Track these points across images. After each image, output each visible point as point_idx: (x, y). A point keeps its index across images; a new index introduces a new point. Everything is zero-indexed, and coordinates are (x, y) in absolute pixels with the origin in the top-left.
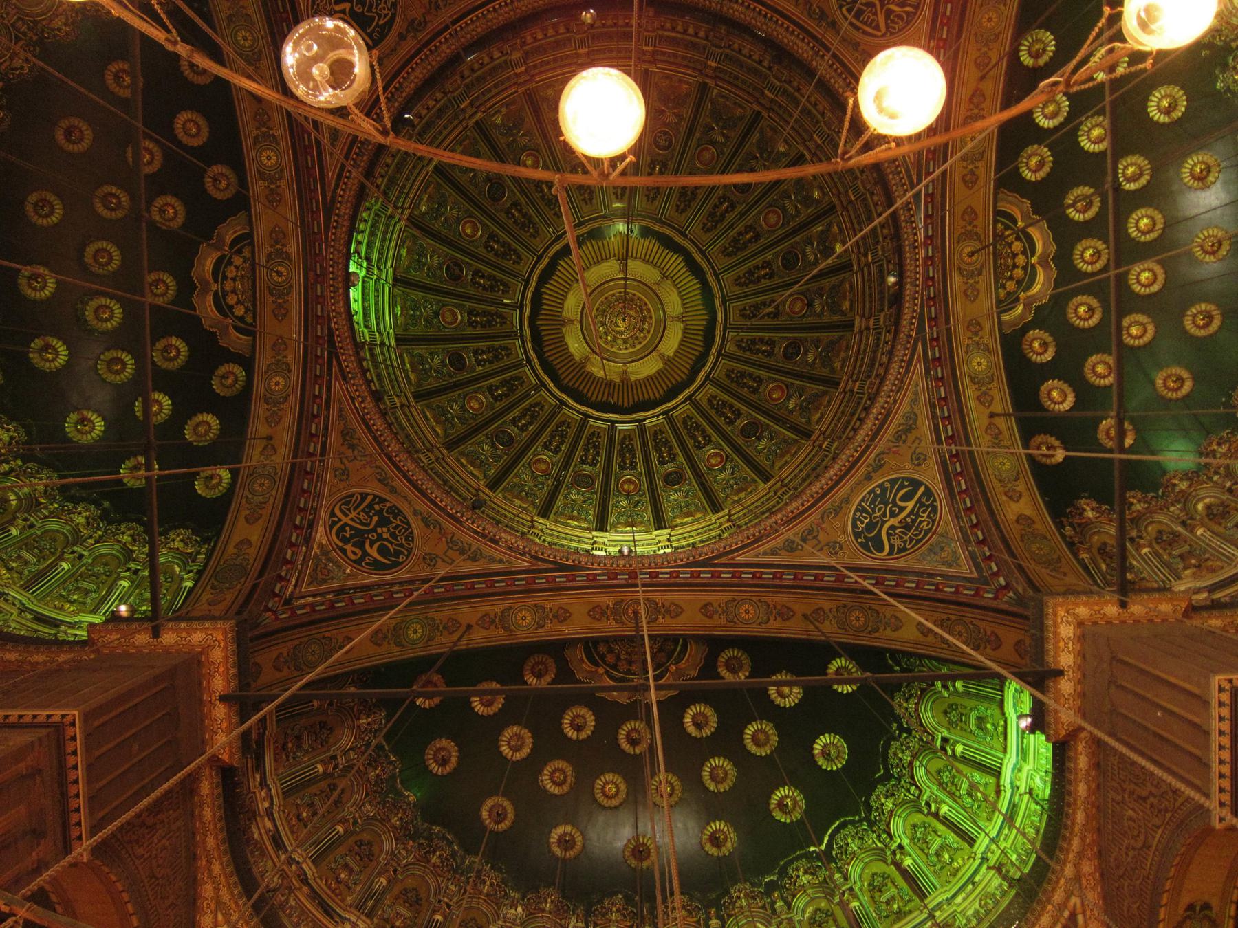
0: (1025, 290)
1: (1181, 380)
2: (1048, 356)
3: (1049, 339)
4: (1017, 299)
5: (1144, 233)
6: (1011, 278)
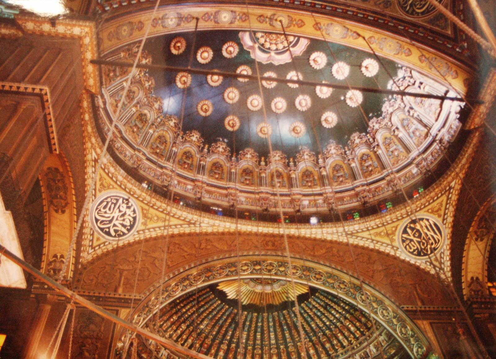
0: (259, 48)
1: (206, 111)
2: (225, 54)
3: (233, 56)
5: (275, 104)
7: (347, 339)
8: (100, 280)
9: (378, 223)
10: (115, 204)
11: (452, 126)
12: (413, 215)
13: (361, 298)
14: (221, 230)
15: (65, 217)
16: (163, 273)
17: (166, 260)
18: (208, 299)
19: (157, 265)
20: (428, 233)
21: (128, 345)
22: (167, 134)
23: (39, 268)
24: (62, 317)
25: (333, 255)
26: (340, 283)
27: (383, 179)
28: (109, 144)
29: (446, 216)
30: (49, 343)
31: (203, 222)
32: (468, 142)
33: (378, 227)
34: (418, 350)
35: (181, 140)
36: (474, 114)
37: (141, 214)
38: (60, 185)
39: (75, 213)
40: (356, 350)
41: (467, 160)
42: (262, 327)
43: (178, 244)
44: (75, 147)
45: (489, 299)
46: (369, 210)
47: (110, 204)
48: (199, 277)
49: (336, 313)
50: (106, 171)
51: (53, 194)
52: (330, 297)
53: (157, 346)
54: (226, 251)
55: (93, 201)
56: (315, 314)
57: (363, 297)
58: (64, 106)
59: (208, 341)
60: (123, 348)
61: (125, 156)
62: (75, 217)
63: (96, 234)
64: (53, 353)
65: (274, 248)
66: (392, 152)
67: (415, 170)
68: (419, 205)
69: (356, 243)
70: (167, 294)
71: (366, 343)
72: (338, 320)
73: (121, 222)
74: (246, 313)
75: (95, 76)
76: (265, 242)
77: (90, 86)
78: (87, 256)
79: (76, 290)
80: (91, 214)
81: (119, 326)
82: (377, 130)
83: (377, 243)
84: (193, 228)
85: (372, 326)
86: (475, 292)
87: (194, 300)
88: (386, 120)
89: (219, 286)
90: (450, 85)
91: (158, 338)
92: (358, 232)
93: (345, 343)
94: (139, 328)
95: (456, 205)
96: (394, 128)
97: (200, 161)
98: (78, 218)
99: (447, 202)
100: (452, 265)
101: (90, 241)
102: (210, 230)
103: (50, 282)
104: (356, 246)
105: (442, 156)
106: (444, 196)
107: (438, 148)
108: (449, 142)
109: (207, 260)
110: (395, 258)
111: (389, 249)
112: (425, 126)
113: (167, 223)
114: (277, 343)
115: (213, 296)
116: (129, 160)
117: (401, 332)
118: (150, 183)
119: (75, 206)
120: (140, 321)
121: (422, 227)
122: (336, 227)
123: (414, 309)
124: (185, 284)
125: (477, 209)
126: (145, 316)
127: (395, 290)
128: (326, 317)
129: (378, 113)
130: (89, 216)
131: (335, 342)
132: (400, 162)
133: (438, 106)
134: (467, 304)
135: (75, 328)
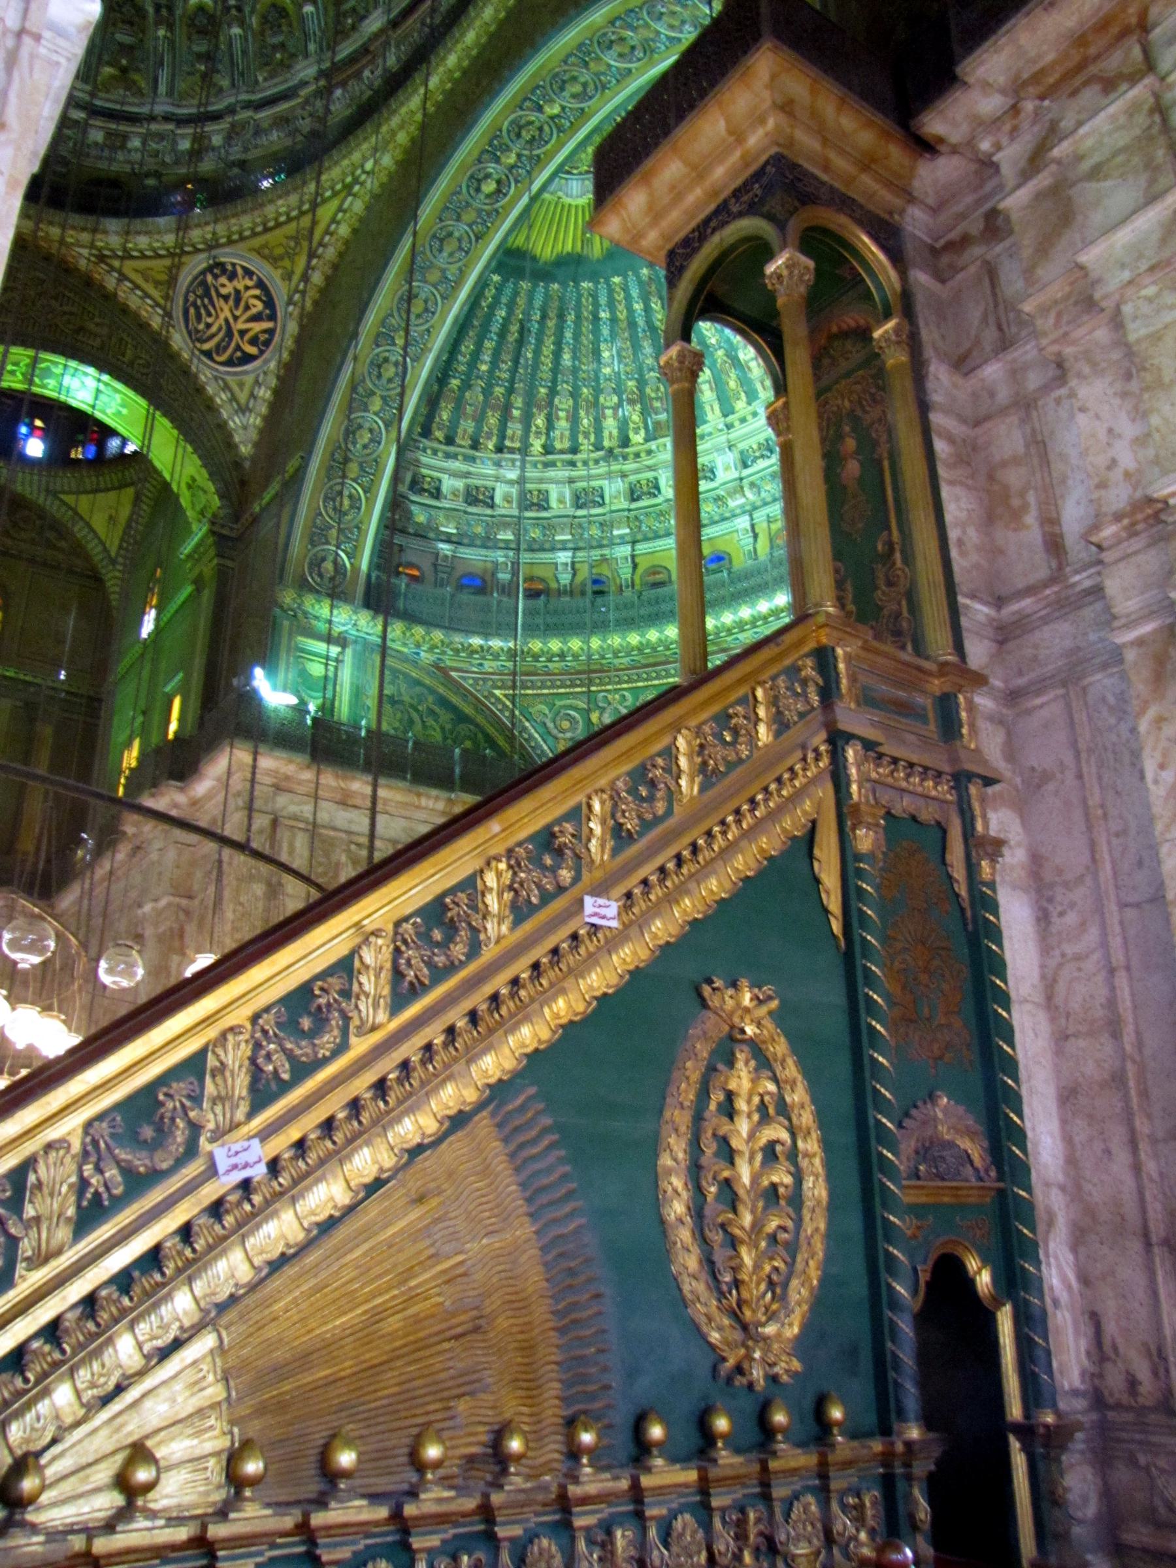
47: (199, 302)
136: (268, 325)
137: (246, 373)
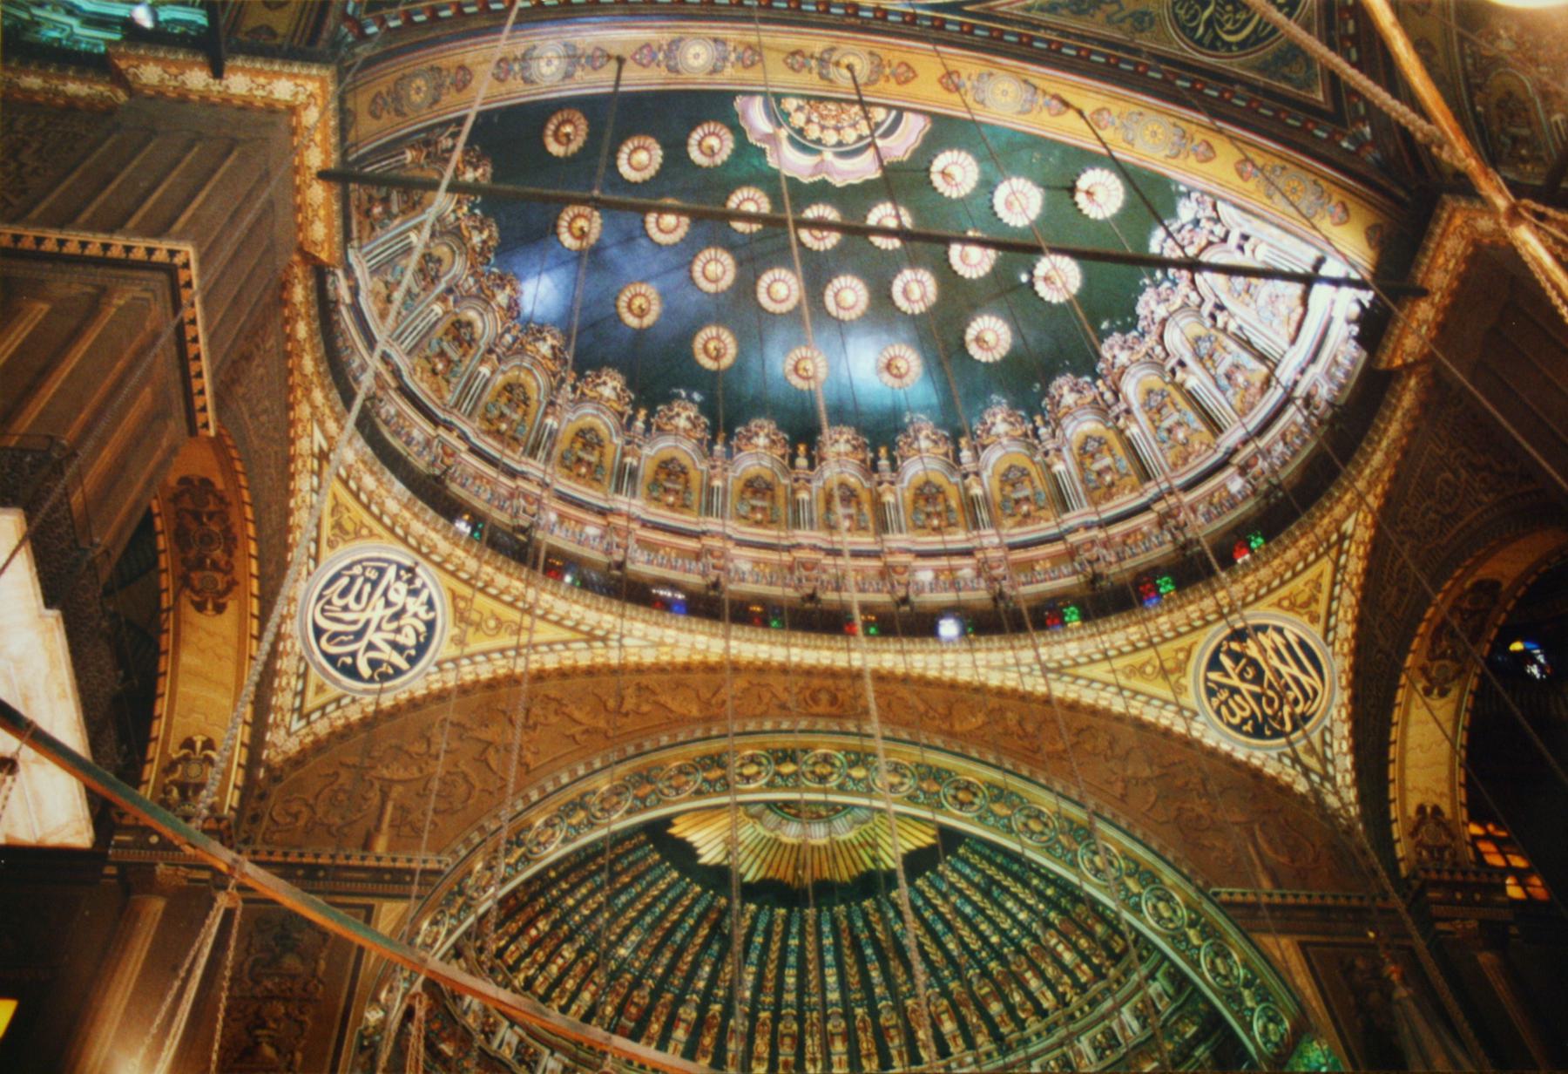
1: (642, 313)
2: (695, 155)
3: (718, 160)
4: (779, 125)
5: (836, 295)
6: (809, 121)
7: (1053, 988)
8: (320, 813)
9: (1134, 638)
10: (375, 584)
11: (1340, 358)
12: (1236, 616)
13: (1092, 862)
14: (681, 657)
15: (225, 624)
16: (511, 788)
17: (521, 748)
18: (642, 868)
19: (493, 764)
20: (1283, 669)
21: (400, 1015)
22: (529, 379)
23: (136, 781)
24: (196, 935)
25: (1007, 733)
26: (1028, 817)
27: (1145, 508)
28: (364, 407)
29: (1333, 621)
30: (151, 1022)
31: (630, 634)
32: (1389, 405)
33: (1136, 649)
34: (1265, 1027)
35: (571, 396)
36: (1400, 324)
37: (450, 610)
38: (215, 528)
39: (256, 611)
40: (1081, 1023)
41: (1387, 454)
42: (802, 948)
43: (554, 699)
44: (264, 418)
45: (1477, 874)
46: (1107, 600)
47: (360, 581)
48: (615, 799)
49: (1020, 905)
50: (353, 485)
51: (192, 554)
52: (999, 859)
53: (488, 1017)
54: (696, 721)
55: (309, 574)
56: (957, 911)
57: (1097, 859)
58: (237, 300)
59: (641, 997)
60: (382, 1025)
61: (408, 443)
62: (255, 624)
63: (314, 673)
64: (164, 1054)
65: (834, 710)
66: (1170, 431)
67: (1236, 485)
68: (1253, 587)
69: (1072, 696)
70: (519, 852)
71: (1108, 1004)
72: (1025, 929)
73: (391, 636)
74: (753, 907)
75: (328, 215)
76: (807, 693)
77: (315, 244)
78: (285, 740)
79: (248, 849)
80: (304, 612)
81: (374, 955)
82: (1124, 369)
83: (1133, 698)
84: (600, 651)
85: (1126, 950)
86: (1431, 853)
87: (601, 869)
88: (1150, 340)
89: (672, 825)
90: (1328, 241)
91: (490, 989)
92: (1077, 664)
93: (1048, 1001)
94: (434, 962)
95: (1362, 587)
96: (1172, 362)
97: (624, 455)
98: (262, 628)
99: (1334, 576)
100: (1356, 766)
101: (296, 694)
102: (649, 657)
103: (165, 826)
104: (1074, 707)
105: (1312, 445)
106: (1325, 559)
107: (1300, 419)
108: (1331, 404)
109: (639, 746)
110: (1188, 743)
111: (1170, 715)
112: (1262, 357)
113: (524, 638)
114: (845, 1000)
115: (657, 857)
116: (419, 454)
117: (1213, 968)
118: (477, 519)
119: (255, 590)
120: (437, 938)
121: (1263, 650)
122: (1012, 648)
123: (1251, 898)
124: (574, 821)
125: (1428, 601)
126: (454, 922)
127: (1189, 839)
128: (990, 920)
129: (1127, 320)
130: (297, 622)
131: (1017, 998)
132: (1192, 461)
133: (1297, 302)
134: (1410, 887)
135: (238, 967)
136: (401, 662)
137: (336, 682)
